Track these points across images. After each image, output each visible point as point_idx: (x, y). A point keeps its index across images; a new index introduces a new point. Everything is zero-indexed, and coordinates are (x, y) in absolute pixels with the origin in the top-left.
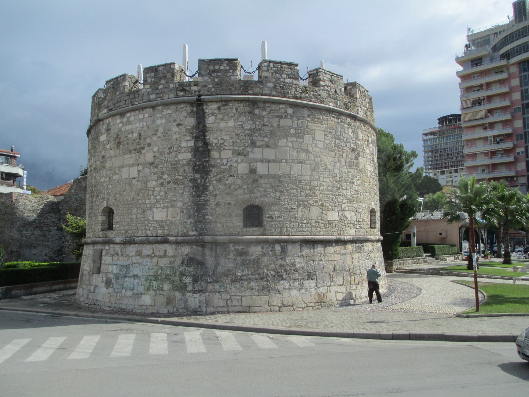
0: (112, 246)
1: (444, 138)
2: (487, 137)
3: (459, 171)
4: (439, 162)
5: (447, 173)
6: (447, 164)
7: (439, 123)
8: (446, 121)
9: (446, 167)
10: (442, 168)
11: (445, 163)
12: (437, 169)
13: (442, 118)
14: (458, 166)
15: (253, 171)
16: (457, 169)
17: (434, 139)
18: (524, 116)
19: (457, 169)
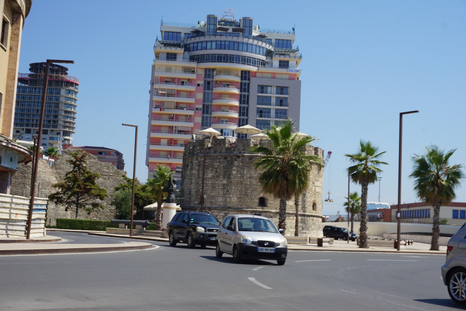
0: (268, 213)
1: (35, 89)
2: (173, 127)
3: (49, 132)
4: (25, 117)
5: (33, 133)
6: (35, 122)
7: (30, 69)
8: (41, 69)
9: (33, 125)
10: (27, 125)
11: (33, 120)
12: (21, 125)
13: (37, 64)
14: (48, 126)
15: (315, 190)
16: (47, 130)
17: (22, 87)
18: (203, 115)
19: (47, 130)
